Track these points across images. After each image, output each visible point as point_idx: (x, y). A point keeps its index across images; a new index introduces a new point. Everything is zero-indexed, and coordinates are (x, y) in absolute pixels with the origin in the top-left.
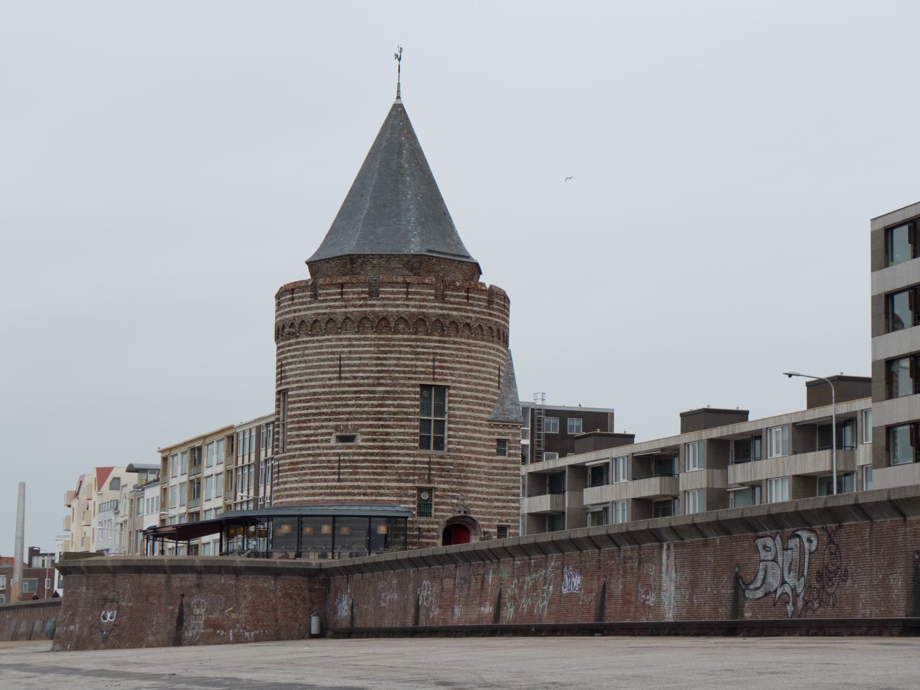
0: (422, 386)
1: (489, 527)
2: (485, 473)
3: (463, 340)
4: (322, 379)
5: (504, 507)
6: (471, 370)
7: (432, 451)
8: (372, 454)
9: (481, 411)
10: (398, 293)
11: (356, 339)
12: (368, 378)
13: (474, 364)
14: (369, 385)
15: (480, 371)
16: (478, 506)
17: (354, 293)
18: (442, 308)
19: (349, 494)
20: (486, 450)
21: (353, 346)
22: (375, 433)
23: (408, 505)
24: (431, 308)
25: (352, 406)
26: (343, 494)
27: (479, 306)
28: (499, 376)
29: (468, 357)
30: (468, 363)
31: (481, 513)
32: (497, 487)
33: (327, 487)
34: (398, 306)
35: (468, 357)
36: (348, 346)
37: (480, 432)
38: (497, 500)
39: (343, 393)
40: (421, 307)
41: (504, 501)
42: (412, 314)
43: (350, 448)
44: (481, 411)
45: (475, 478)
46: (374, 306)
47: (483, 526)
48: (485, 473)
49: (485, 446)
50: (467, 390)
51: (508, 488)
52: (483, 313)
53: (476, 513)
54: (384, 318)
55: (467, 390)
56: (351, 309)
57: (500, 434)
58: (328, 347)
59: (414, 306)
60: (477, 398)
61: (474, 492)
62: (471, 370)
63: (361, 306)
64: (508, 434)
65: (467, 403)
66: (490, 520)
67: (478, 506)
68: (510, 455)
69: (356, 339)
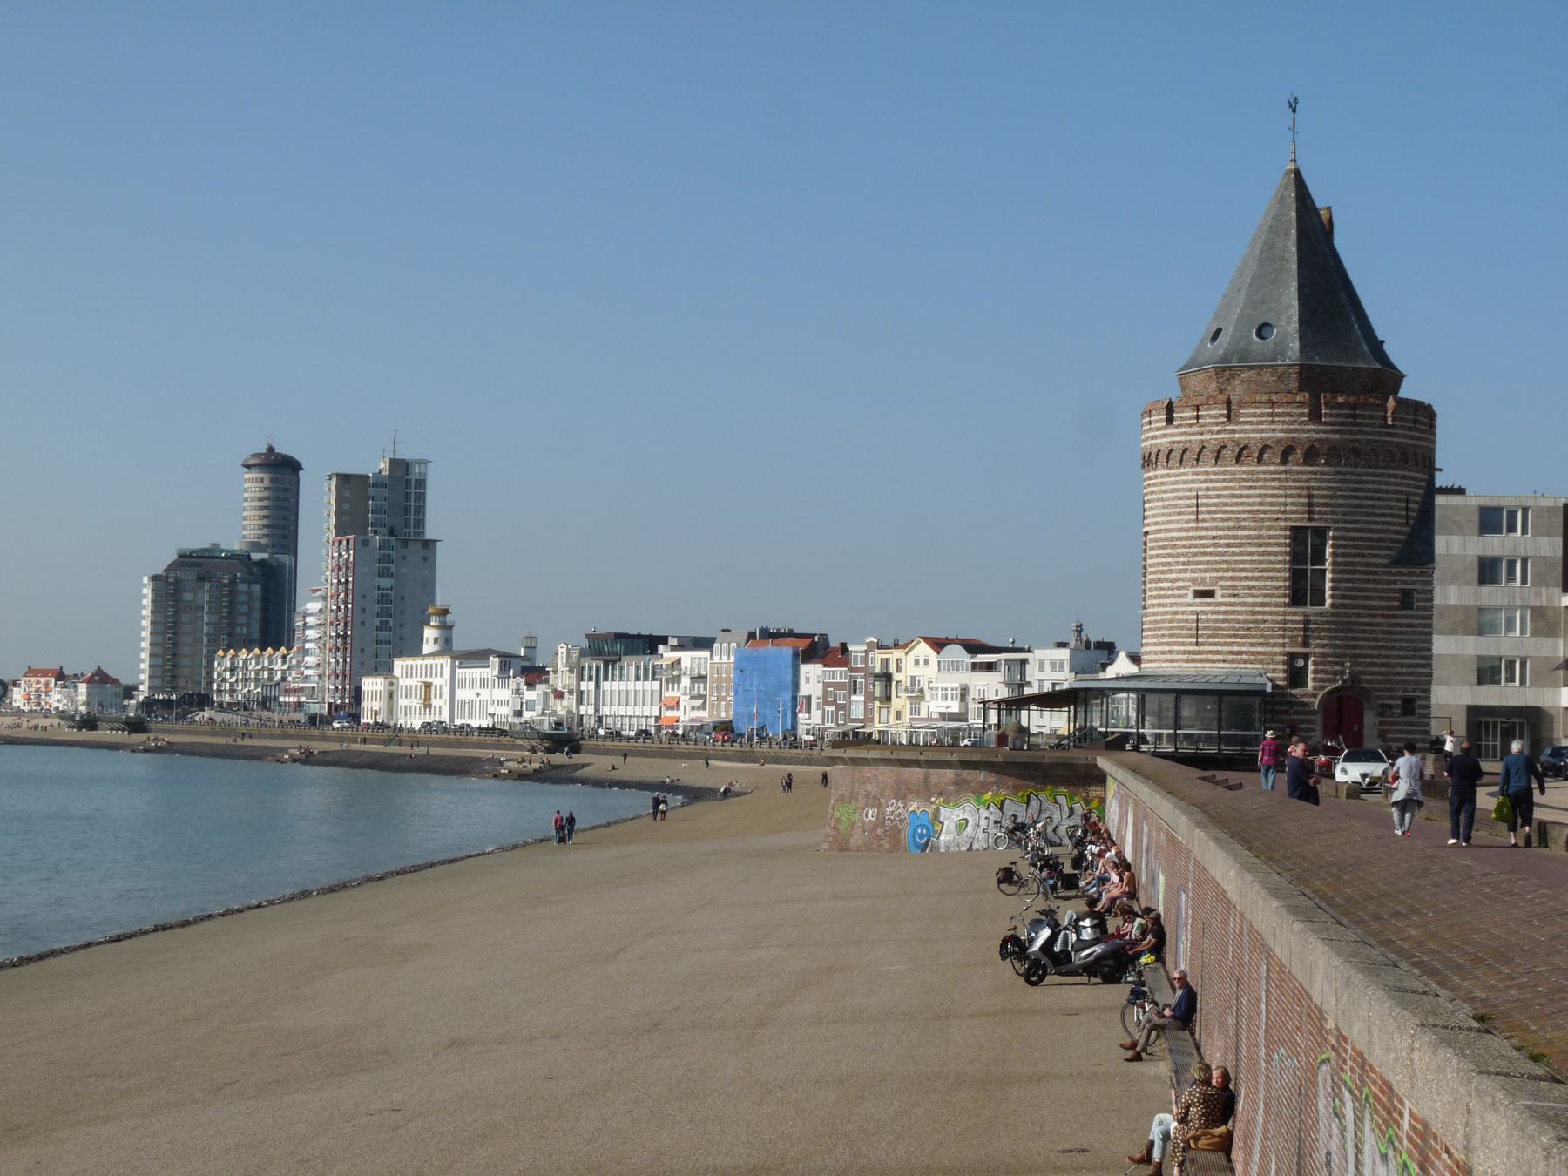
0: (1292, 528)
1: (1389, 698)
2: (1383, 632)
3: (1349, 469)
4: (1178, 522)
5: (1411, 674)
6: (1360, 506)
7: (1309, 609)
8: (1234, 612)
9: (1376, 556)
10: (1261, 415)
11: (1215, 473)
12: (1227, 520)
13: (1366, 498)
14: (1229, 529)
15: (1374, 507)
16: (1372, 673)
17: (1210, 416)
18: (1318, 432)
19: (1207, 661)
20: (1384, 603)
21: (1212, 481)
22: (1234, 587)
23: (1279, 673)
24: (1303, 431)
25: (1211, 554)
26: (1201, 661)
27: (1372, 425)
28: (1407, 509)
29: (1357, 490)
30: (1356, 497)
31: (1377, 681)
32: (1401, 648)
33: (1185, 652)
34: (1262, 431)
35: (1357, 490)
36: (1206, 481)
37: (1374, 581)
38: (1401, 665)
39: (1201, 538)
40: (1291, 431)
41: (1410, 666)
42: (1279, 441)
43: (1209, 604)
44: (1376, 556)
45: (1368, 639)
46: (1234, 431)
47: (1379, 697)
48: (1383, 632)
49: (1382, 599)
50: (1355, 530)
51: (1416, 649)
52: (1379, 434)
53: (1370, 682)
54: (1245, 447)
55: (1355, 530)
56: (1208, 437)
57: (1404, 582)
58: (1184, 482)
59: (1283, 431)
60: (1370, 540)
61: (1366, 656)
62: (1360, 506)
63: (1219, 432)
64: (1415, 583)
65: (1355, 547)
66: (1391, 690)
67: (1372, 673)
68: (1419, 608)
69: (1215, 473)
